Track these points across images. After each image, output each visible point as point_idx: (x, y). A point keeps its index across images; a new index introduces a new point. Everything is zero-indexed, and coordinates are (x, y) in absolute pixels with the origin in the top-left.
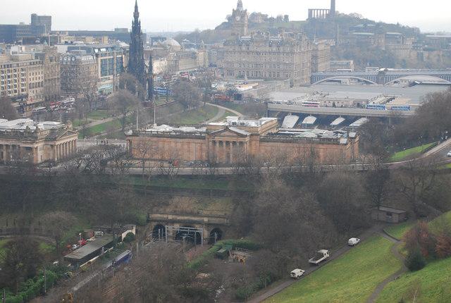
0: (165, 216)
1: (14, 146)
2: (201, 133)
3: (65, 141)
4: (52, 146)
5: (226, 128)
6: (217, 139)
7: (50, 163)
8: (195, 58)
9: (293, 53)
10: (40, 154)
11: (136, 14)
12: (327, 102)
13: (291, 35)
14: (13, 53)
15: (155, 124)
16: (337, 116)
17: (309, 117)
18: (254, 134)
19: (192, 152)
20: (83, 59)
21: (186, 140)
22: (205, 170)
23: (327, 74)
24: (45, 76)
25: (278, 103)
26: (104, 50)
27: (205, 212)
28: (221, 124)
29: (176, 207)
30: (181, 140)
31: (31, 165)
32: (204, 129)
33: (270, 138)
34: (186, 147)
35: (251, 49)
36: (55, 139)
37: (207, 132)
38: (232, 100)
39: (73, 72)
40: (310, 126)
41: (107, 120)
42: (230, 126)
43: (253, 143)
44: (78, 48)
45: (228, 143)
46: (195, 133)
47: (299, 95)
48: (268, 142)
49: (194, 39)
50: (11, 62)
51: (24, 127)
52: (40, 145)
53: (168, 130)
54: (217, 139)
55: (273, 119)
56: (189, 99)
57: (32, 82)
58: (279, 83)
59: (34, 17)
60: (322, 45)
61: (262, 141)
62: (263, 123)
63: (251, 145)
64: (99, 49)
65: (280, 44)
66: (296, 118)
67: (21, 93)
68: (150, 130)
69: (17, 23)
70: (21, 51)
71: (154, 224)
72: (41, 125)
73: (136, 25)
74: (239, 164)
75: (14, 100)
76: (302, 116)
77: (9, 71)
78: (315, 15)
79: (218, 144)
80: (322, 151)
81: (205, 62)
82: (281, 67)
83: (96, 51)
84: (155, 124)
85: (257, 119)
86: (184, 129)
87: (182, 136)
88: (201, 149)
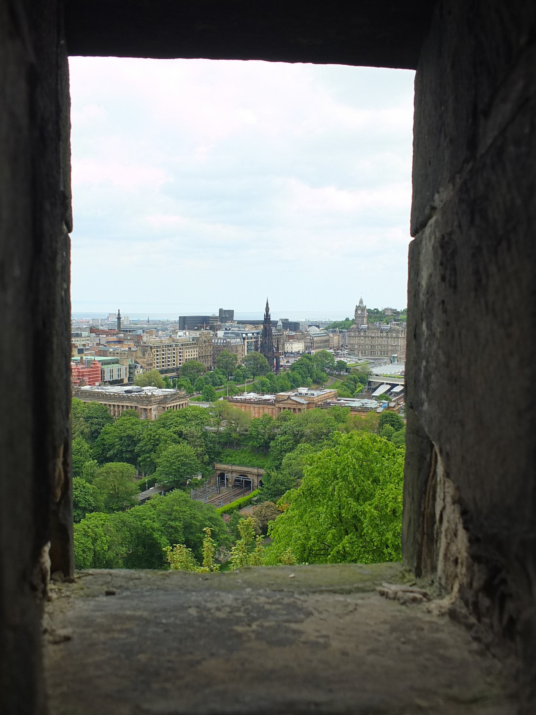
1: (136, 407)
3: (172, 405)
4: (164, 408)
5: (289, 397)
6: (281, 405)
9: (397, 337)
14: (179, 336)
17: (398, 387)
24: (199, 353)
26: (251, 335)
30: (257, 406)
34: (261, 411)
36: (165, 403)
42: (296, 395)
44: (228, 333)
52: (153, 407)
54: (281, 405)
55: (333, 390)
57: (188, 357)
59: (221, 310)
64: (246, 334)
65: (391, 330)
66: (389, 387)
67: (179, 365)
71: (219, 472)
73: (267, 316)
79: (282, 410)
82: (390, 348)
83: (244, 335)
84: (246, 393)
86: (267, 397)
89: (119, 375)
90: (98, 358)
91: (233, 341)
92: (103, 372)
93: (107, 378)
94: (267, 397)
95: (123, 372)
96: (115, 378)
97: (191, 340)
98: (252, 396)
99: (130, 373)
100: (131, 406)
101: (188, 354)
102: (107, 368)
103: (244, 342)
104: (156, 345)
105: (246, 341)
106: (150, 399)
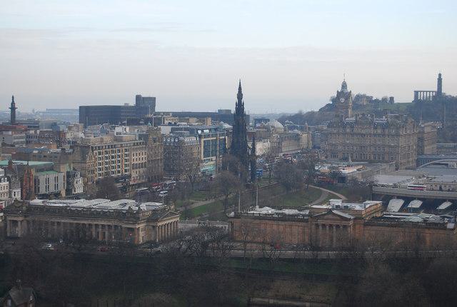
0: (266, 300)
1: (116, 227)
2: (304, 216)
3: (167, 222)
4: (154, 227)
5: (330, 211)
6: (320, 222)
7: (151, 243)
8: (299, 139)
9: (398, 135)
10: (141, 237)
11: (240, 96)
12: (434, 186)
13: (397, 117)
14: (117, 134)
15: (257, 207)
16: (444, 201)
17: (415, 201)
18: (358, 217)
19: (295, 235)
20: (187, 140)
21: (290, 223)
22: (308, 254)
23: (434, 157)
24: (148, 157)
25: (383, 186)
27: (307, 297)
28: (324, 207)
29: (278, 291)
30: (283, 223)
31: (132, 246)
32: (307, 212)
33: (374, 221)
35: (355, 131)
36: (157, 220)
37: (310, 215)
38: (336, 182)
39: (176, 153)
40: (415, 210)
41: (208, 202)
42: (333, 209)
43: (357, 226)
44: (181, 129)
45: (331, 226)
46: (298, 215)
47: (404, 178)
48: (372, 226)
49: (298, 121)
50: (115, 143)
51: (127, 208)
52: (141, 226)
53: (270, 212)
54: (320, 222)
55: (378, 202)
56: (294, 181)
57: (135, 162)
58: (385, 166)
59: (138, 98)
60: (428, 127)
61: (366, 225)
62: (367, 206)
63: (354, 229)
64: (202, 131)
65: (385, 126)
66: (401, 202)
67: (124, 173)
68: (252, 212)
69: (122, 104)
70: (125, 132)
72: (143, 206)
73: (240, 106)
74: (343, 249)
75: (117, 180)
76: (408, 199)
77: (113, 152)
78: (421, 96)
79: (321, 228)
80: (429, 236)
81: (308, 141)
84: (257, 207)
85: (361, 202)
86: (287, 211)
87: (285, 218)
88: (304, 233)
89: (56, 186)
90: (31, 163)
91: (187, 140)
92: (37, 181)
93: (43, 191)
94: (287, 211)
95: (61, 181)
96: (52, 189)
97: (137, 138)
98: (267, 210)
99: (68, 183)
100: (109, 226)
101: (135, 157)
102: (42, 177)
103: (200, 141)
104: (97, 145)
105: (203, 140)
106: (137, 216)
